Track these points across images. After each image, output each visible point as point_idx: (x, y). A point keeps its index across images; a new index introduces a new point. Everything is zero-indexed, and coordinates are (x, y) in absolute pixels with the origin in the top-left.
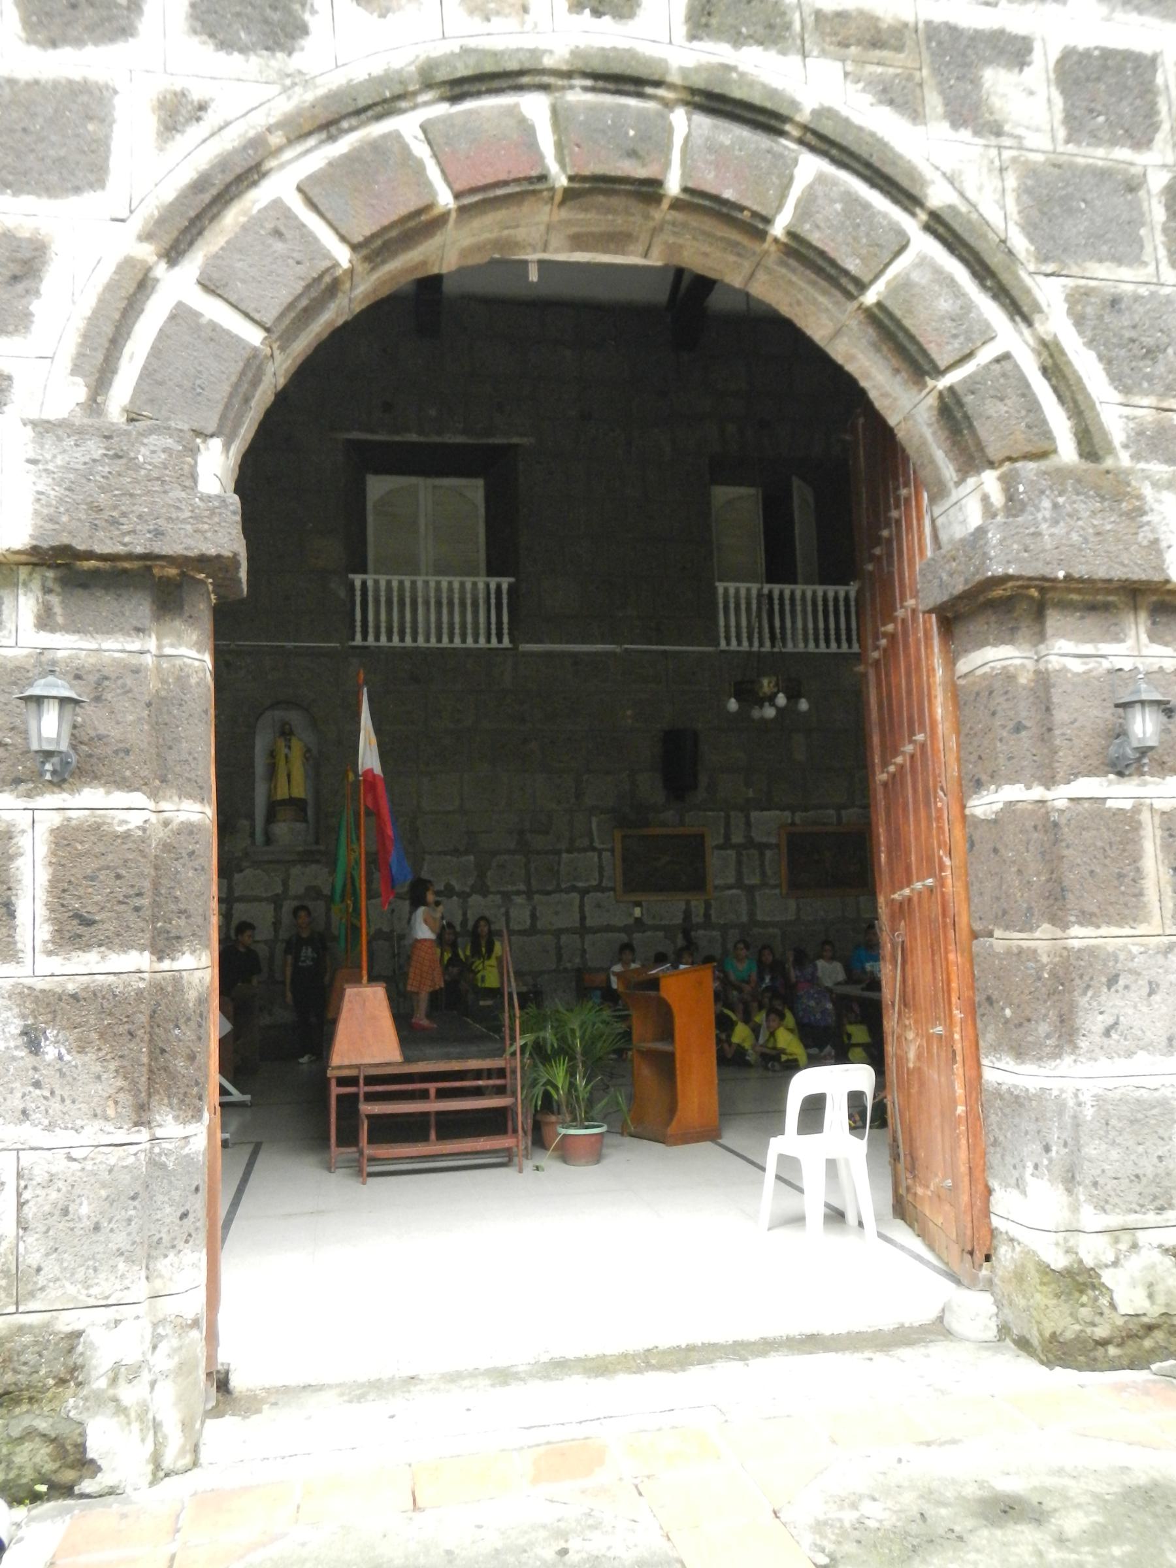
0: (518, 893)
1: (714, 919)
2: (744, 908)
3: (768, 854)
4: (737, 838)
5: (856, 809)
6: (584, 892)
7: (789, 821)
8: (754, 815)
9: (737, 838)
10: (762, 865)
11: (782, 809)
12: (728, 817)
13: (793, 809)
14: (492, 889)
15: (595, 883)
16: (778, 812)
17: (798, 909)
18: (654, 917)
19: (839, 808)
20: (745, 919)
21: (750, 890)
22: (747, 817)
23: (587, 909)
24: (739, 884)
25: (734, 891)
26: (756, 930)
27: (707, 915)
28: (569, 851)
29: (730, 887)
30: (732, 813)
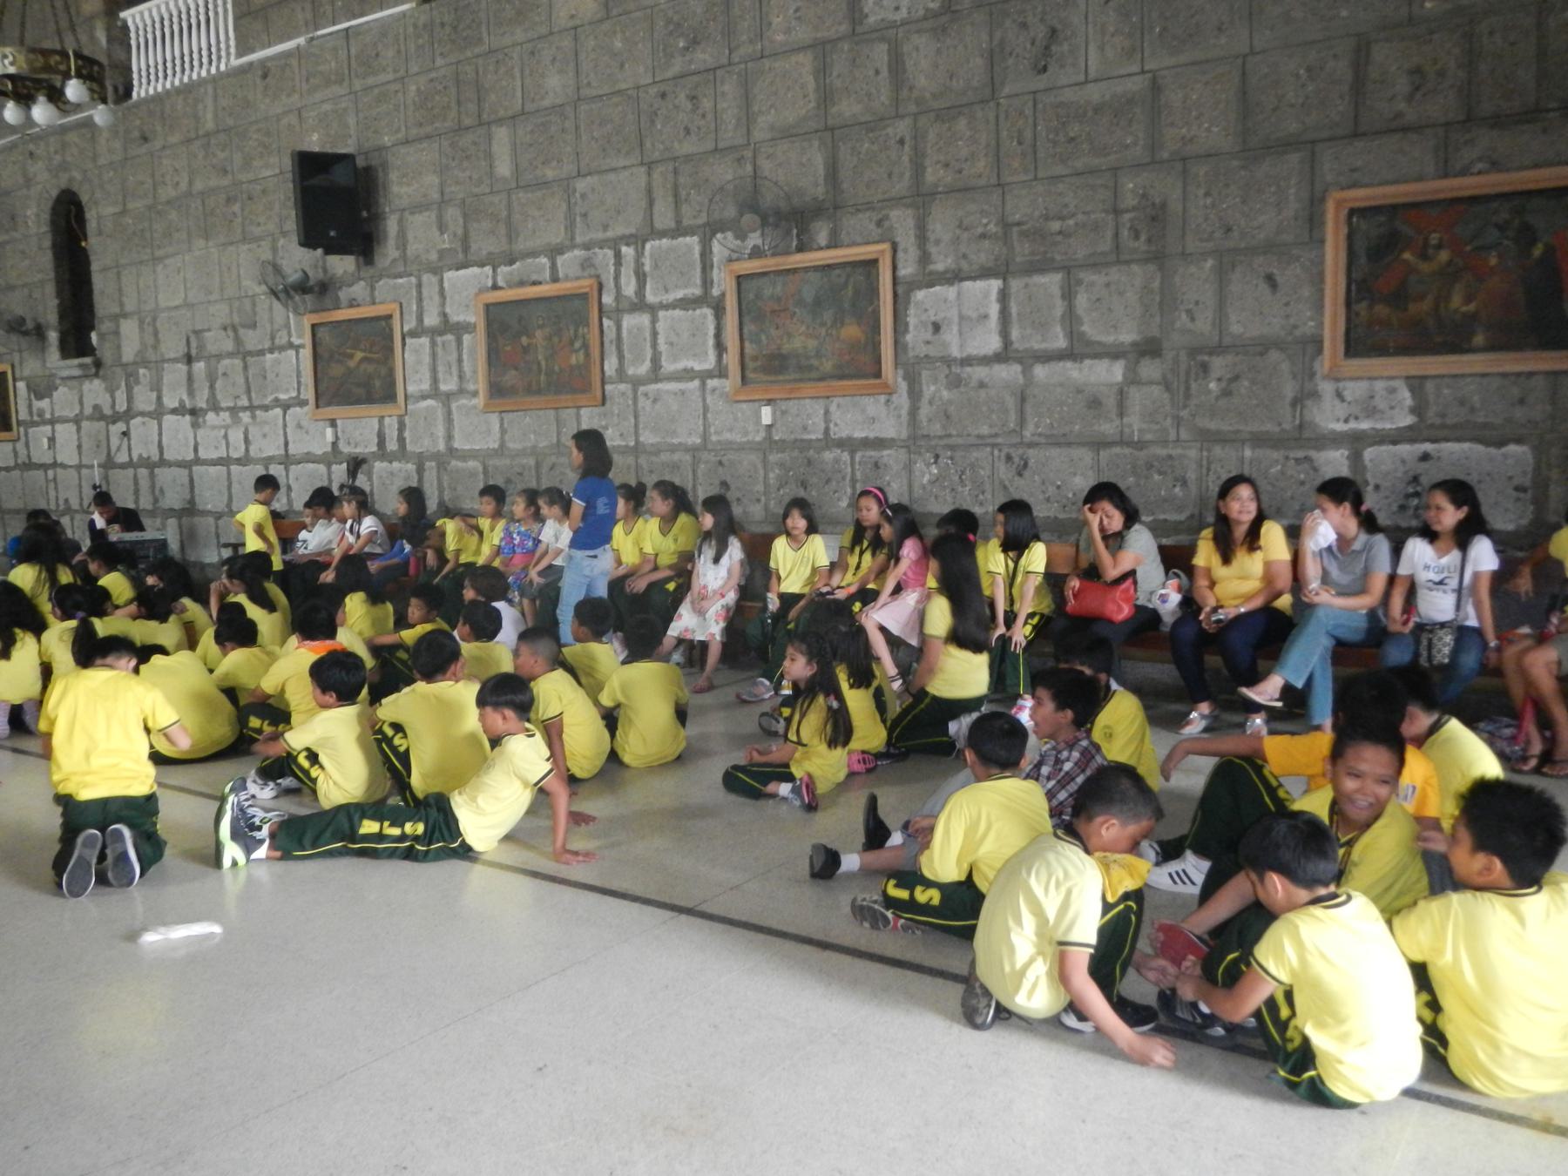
0: (245, 409)
1: (409, 447)
2: (440, 431)
3: (466, 338)
4: (431, 320)
5: (577, 252)
6: (286, 407)
7: (490, 283)
8: (449, 276)
9: (431, 320)
10: (460, 360)
11: (482, 265)
12: (419, 286)
13: (493, 261)
14: (223, 405)
15: (294, 394)
16: (475, 270)
17: (503, 431)
18: (349, 443)
19: (554, 252)
20: (441, 446)
21: (447, 398)
22: (441, 281)
23: (288, 430)
24: (434, 393)
25: (430, 402)
26: (455, 464)
27: (401, 440)
28: (271, 351)
29: (424, 397)
30: (426, 278)
